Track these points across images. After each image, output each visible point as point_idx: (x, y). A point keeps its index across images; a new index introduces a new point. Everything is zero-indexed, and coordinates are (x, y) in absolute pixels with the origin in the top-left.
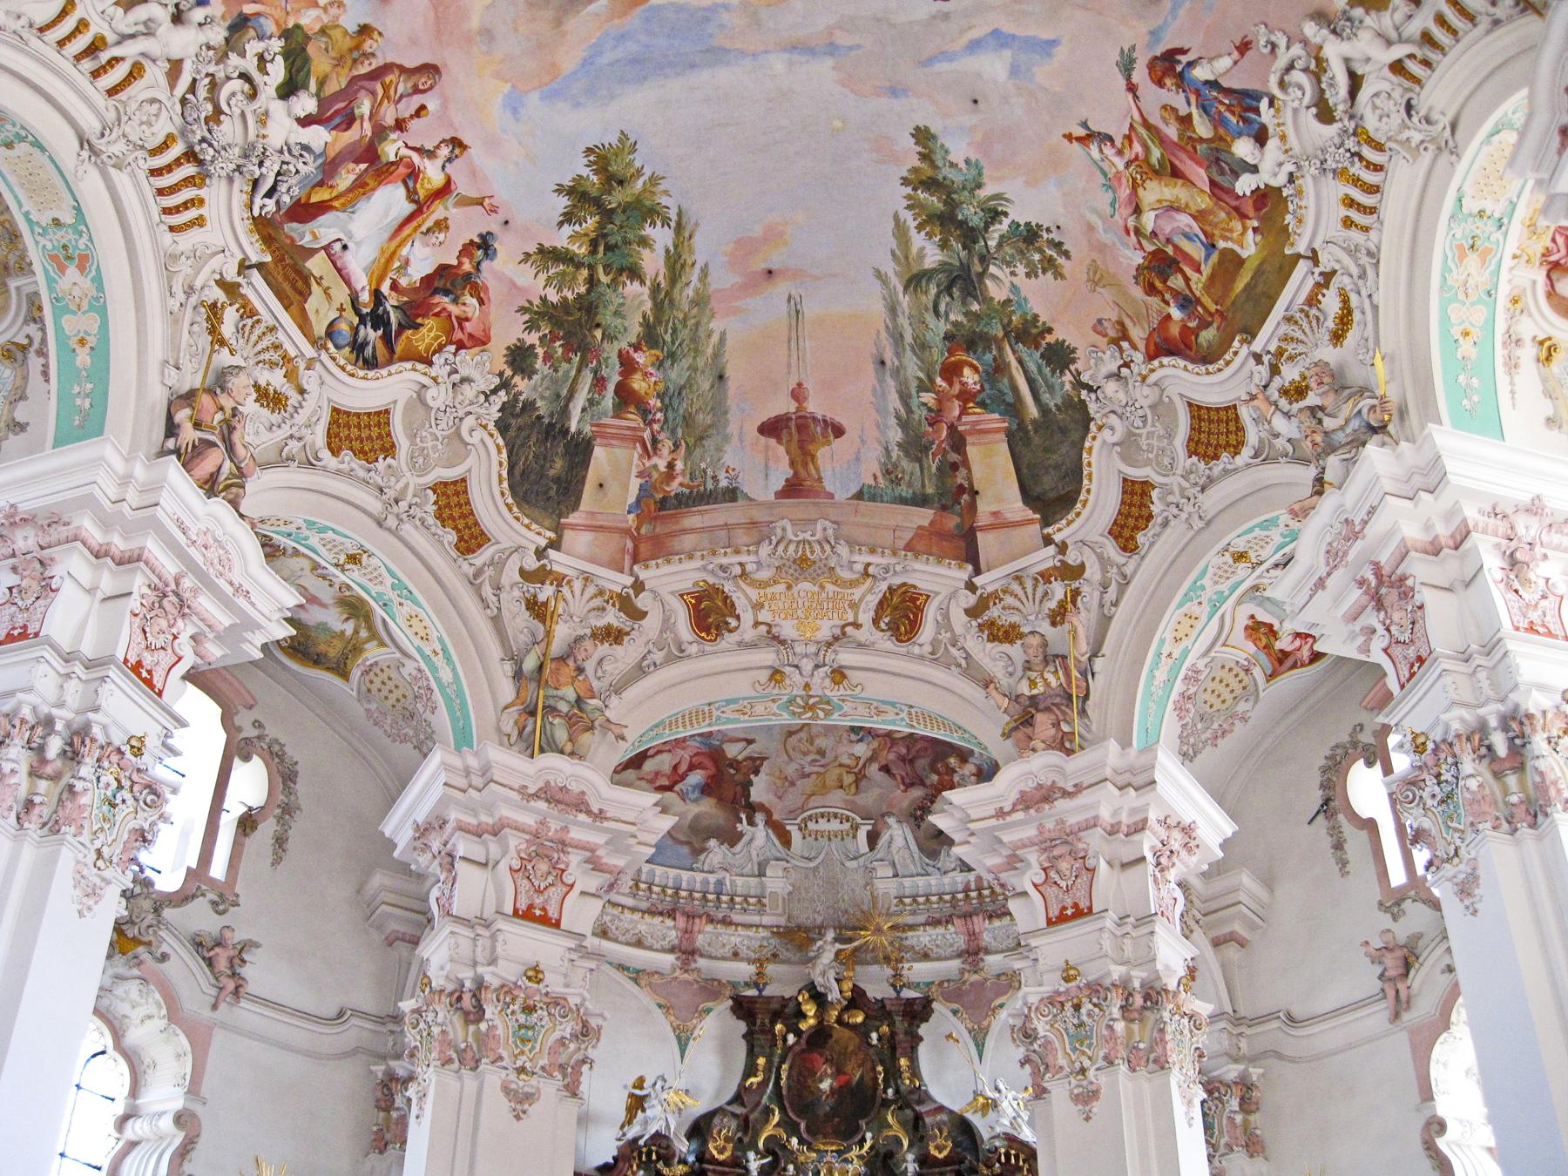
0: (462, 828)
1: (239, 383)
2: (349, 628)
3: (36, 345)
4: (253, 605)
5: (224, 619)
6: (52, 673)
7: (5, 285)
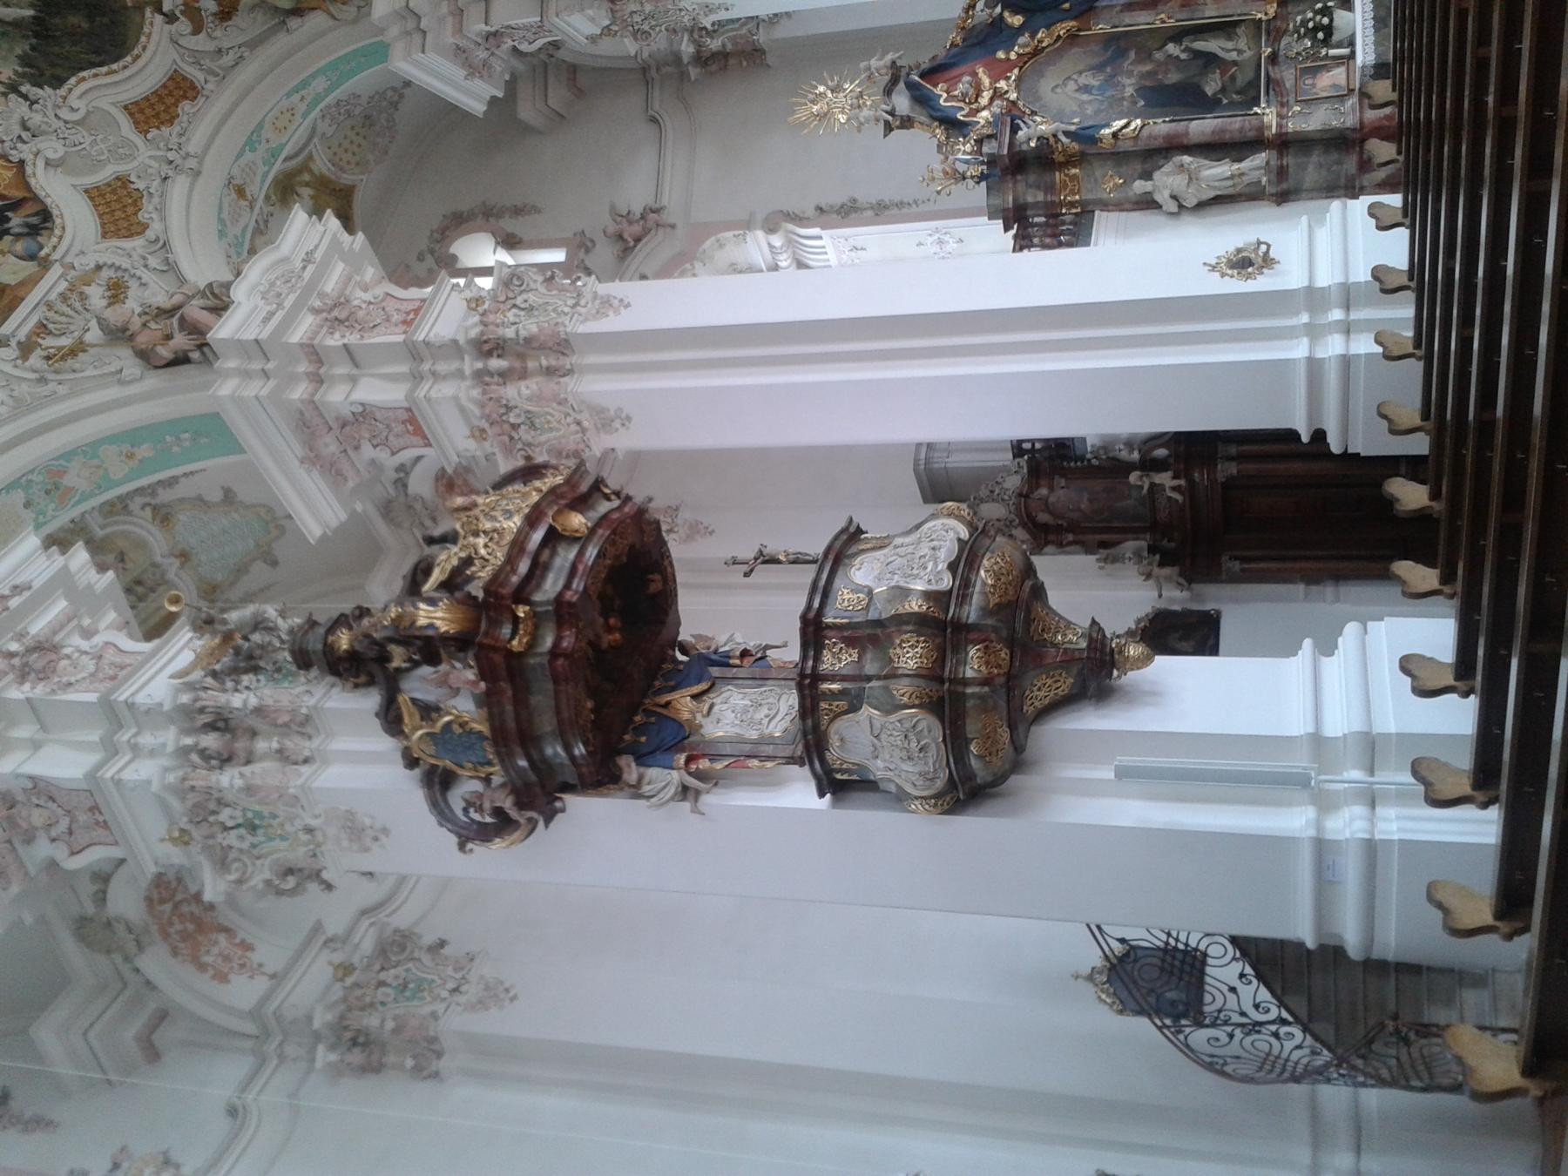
0: (459, 29)
1: (114, 316)
2: (306, 192)
3: (148, 500)
4: (316, 247)
5: (339, 269)
6: (436, 387)
7: (105, 539)
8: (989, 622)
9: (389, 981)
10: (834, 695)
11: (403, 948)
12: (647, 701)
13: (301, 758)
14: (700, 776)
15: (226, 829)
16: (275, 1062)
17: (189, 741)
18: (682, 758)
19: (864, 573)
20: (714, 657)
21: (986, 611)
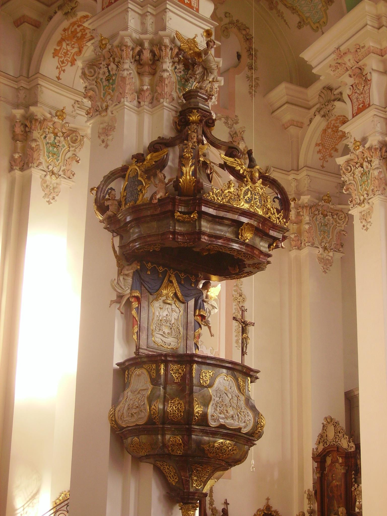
8: (194, 446)
9: (58, 138)
10: (158, 370)
11: (74, 141)
12: (172, 271)
13: (140, 100)
14: (128, 303)
15: (108, 65)
16: (16, 87)
17: (146, 45)
18: (137, 294)
19: (223, 381)
20: (200, 301)
21: (199, 443)
